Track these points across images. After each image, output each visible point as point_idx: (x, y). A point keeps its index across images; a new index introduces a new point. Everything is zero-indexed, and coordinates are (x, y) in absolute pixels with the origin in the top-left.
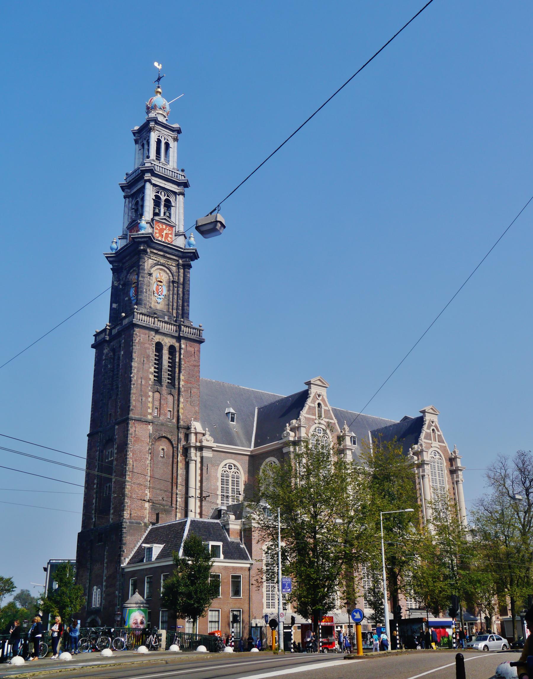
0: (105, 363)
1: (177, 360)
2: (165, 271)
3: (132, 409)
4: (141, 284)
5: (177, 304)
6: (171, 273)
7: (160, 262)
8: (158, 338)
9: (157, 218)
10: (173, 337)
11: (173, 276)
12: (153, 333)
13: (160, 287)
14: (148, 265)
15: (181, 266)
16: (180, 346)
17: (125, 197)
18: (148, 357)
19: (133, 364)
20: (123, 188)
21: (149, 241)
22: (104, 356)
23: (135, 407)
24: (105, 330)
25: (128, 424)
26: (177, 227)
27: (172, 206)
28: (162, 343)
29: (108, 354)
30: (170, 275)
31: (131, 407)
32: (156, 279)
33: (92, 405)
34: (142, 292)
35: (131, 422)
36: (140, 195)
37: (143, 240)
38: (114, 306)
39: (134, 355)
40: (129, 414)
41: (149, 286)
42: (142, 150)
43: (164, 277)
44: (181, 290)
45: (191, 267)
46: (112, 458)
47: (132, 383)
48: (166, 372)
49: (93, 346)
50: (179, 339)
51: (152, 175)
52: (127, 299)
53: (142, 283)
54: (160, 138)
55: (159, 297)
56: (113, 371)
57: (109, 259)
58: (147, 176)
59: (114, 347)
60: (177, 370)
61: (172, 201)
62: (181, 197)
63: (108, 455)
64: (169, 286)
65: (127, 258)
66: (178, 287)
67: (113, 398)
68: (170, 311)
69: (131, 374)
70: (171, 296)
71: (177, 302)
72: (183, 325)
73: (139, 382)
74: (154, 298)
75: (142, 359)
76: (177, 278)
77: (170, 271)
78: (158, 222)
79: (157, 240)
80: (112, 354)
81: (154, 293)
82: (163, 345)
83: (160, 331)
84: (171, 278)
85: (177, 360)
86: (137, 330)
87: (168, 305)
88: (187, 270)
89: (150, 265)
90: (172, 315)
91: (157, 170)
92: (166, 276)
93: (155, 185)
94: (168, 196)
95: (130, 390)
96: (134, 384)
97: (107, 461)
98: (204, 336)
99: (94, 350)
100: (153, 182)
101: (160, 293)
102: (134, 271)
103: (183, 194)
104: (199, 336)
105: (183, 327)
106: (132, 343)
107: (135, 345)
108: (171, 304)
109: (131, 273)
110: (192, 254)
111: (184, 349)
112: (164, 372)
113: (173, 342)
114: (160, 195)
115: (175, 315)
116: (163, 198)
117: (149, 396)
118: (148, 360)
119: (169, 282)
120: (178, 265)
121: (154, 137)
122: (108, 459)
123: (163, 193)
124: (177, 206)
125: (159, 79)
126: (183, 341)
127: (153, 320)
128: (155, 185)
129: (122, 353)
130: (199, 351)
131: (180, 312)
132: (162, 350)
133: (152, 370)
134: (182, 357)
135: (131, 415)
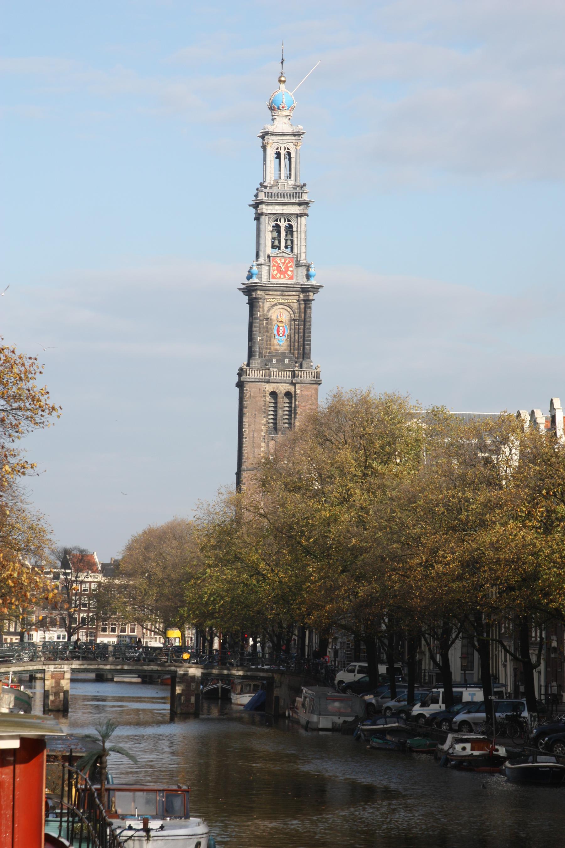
16: (295, 391)
19: (244, 420)
28: (277, 391)
30: (291, 312)
31: (244, 460)
41: (267, 332)
47: (245, 437)
54: (279, 150)
61: (294, 226)
64: (291, 325)
73: (251, 435)
84: (293, 315)
87: (290, 345)
89: (266, 309)
92: (288, 314)
96: (246, 438)
101: (281, 335)
107: (246, 401)
114: (278, 223)
116: (283, 224)
117: (262, 447)
123: (283, 220)
124: (299, 230)
131: (301, 351)
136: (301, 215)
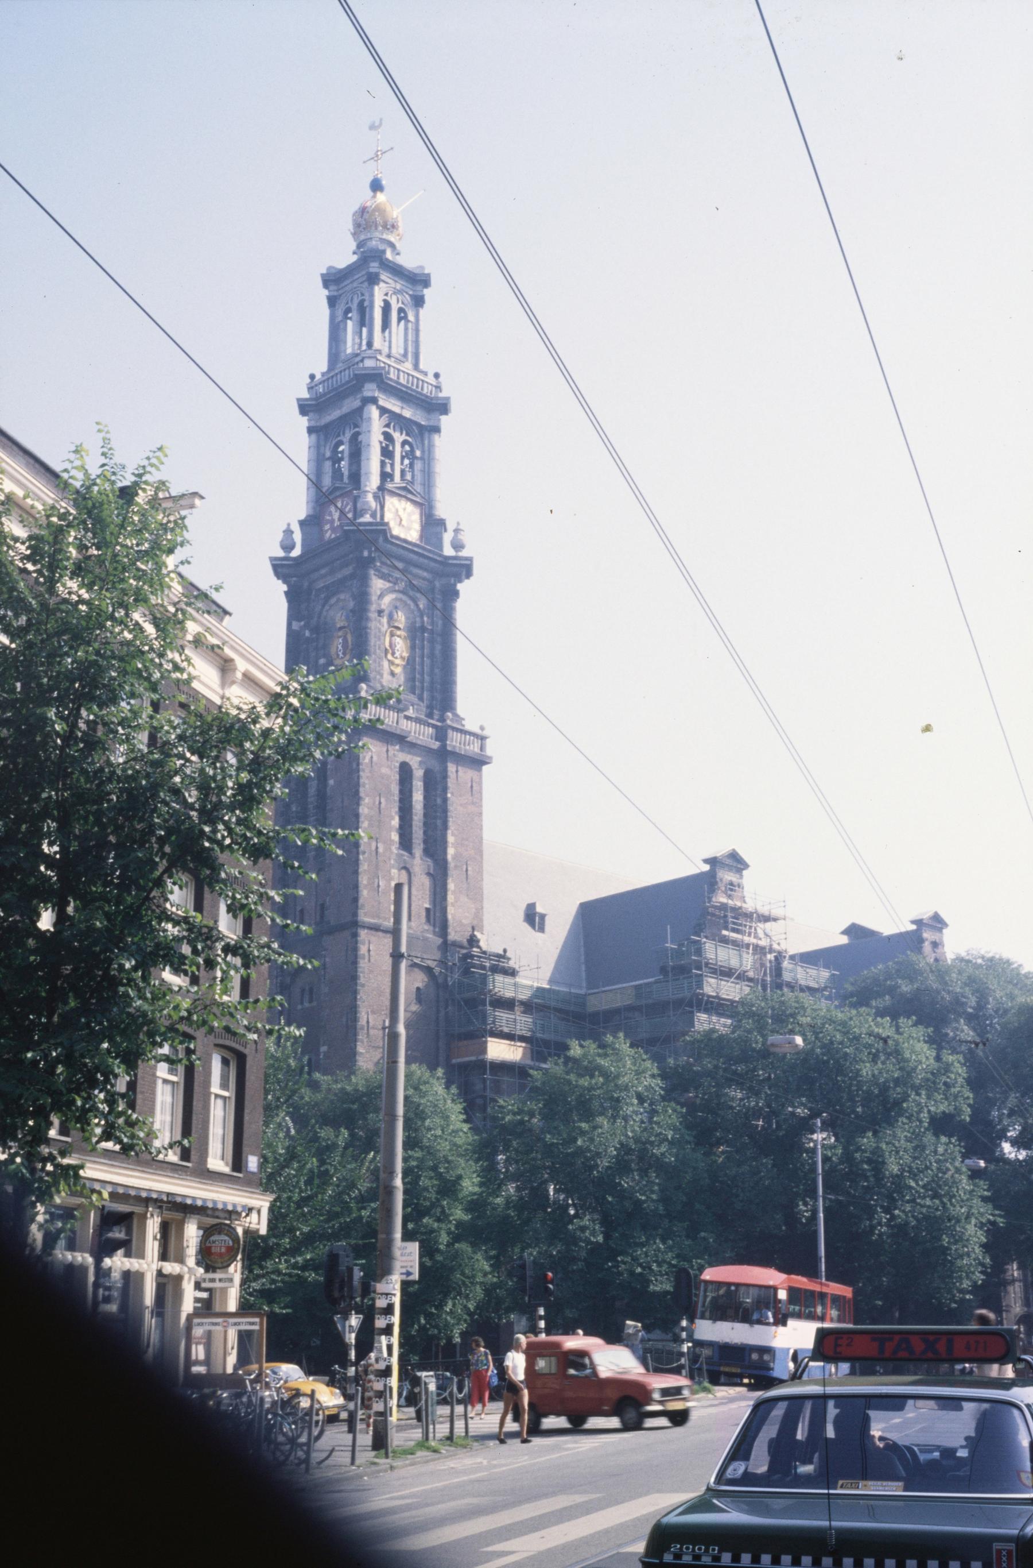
11: (422, 617)
17: (310, 430)
19: (361, 811)
20: (304, 408)
25: (355, 935)
35: (363, 934)
36: (347, 431)
47: (362, 848)
54: (388, 298)
73: (373, 848)
78: (393, 493)
83: (408, 739)
87: (413, 679)
93: (383, 411)
96: (364, 853)
97: (299, 1007)
100: (381, 403)
114: (391, 431)
116: (399, 437)
128: (383, 411)
133: (396, 822)
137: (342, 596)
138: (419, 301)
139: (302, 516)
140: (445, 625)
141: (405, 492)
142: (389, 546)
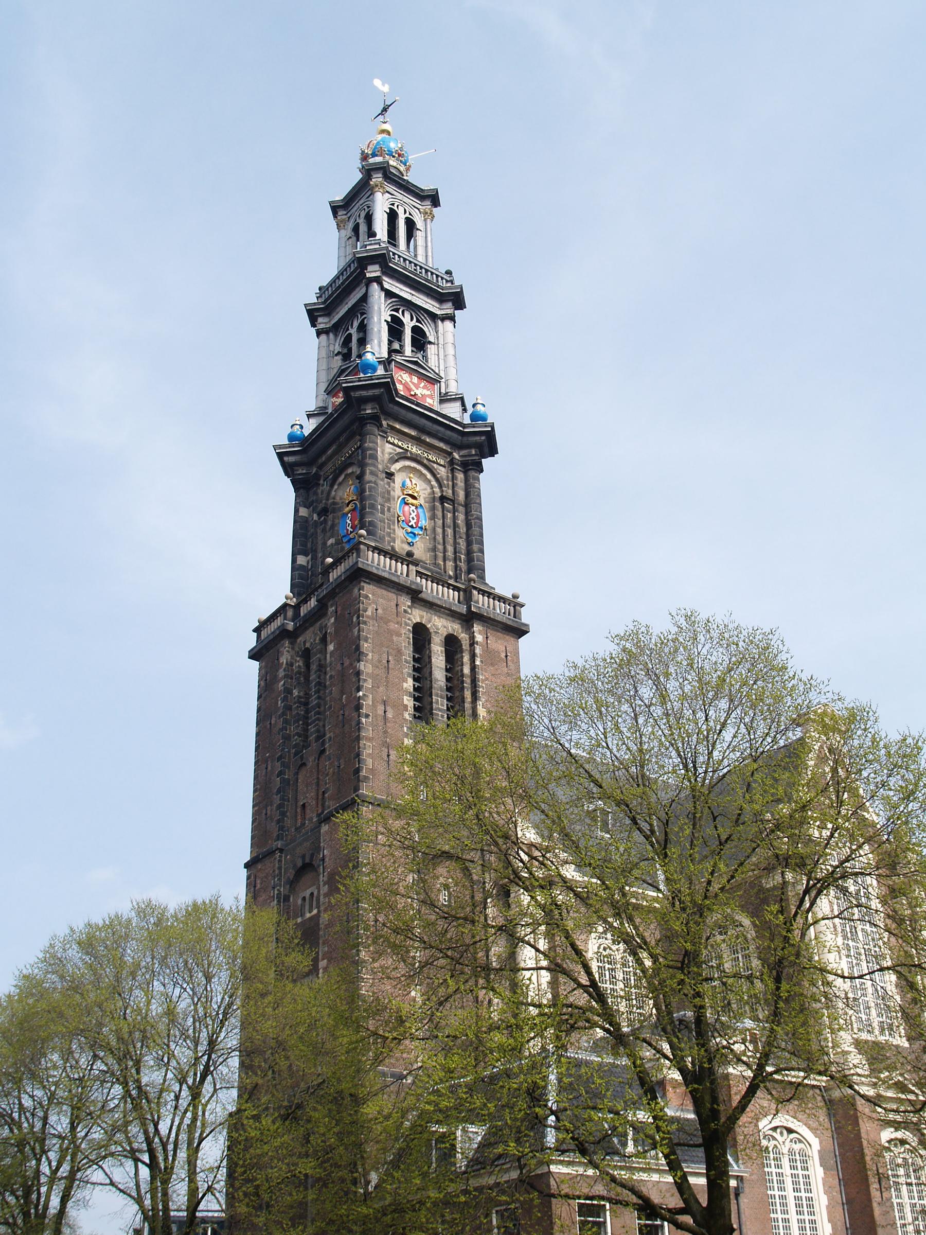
0: (284, 684)
1: (467, 670)
2: (421, 475)
3: (366, 778)
4: (370, 489)
5: (455, 549)
6: (437, 480)
7: (411, 453)
8: (418, 615)
9: (398, 358)
10: (452, 614)
12: (405, 601)
13: (413, 508)
14: (383, 453)
15: (457, 465)
16: (472, 638)
17: (319, 334)
18: (399, 652)
21: (386, 397)
22: (281, 670)
23: (372, 770)
24: (284, 608)
26: (443, 385)
27: (430, 343)
28: (429, 626)
29: (292, 665)
30: (434, 483)
31: (363, 773)
32: (403, 490)
33: (255, 791)
34: (373, 506)
37: (370, 393)
38: (302, 560)
39: (365, 646)
40: (357, 789)
41: (388, 500)
42: (354, 239)
43: (421, 488)
44: (461, 517)
45: (492, 450)
46: (315, 911)
47: (364, 711)
48: (441, 697)
49: (254, 655)
50: (469, 618)
51: (384, 273)
52: (331, 541)
53: (374, 488)
54: (395, 208)
55: (410, 530)
56: (306, 704)
57: (286, 459)
58: (373, 271)
59: (308, 645)
60: (468, 694)
62: (448, 324)
63: (303, 906)
64: (433, 509)
65: (330, 452)
66: (454, 511)
67: (310, 764)
68: (439, 564)
69: (358, 690)
70: (439, 530)
71: (455, 543)
72: (475, 588)
73: (380, 711)
74: (400, 533)
75: (385, 656)
76: (450, 491)
77: (434, 475)
79: (403, 397)
80: (301, 664)
81: (398, 521)
82: (431, 631)
83: (422, 595)
84: (437, 490)
85: (467, 670)
86: (369, 590)
87: (434, 549)
88: (472, 474)
89: (387, 456)
90: (445, 572)
91: (396, 264)
92: (424, 485)
93: (389, 294)
94: (418, 321)
95: (359, 730)
96: (367, 716)
98: (526, 616)
99: (256, 664)
102: (347, 476)
103: (452, 318)
104: (515, 617)
105: (475, 592)
106: (358, 617)
107: (365, 623)
108: (440, 547)
109: (340, 484)
110: (483, 438)
111: (481, 645)
112: (437, 695)
113: (454, 627)
114: (400, 315)
115: (451, 573)
116: (409, 323)
118: (398, 661)
119: (434, 499)
120: (452, 462)
121: (381, 203)
122: (302, 915)
123: (407, 315)
124: (441, 341)
125: (385, 110)
126: (477, 628)
127: (405, 567)
128: (389, 294)
129: (331, 647)
130: (517, 653)
132: (430, 643)
133: (409, 684)
134: (478, 663)
135: (364, 791)
136: (444, 318)
137: (350, 471)
138: (430, 216)
139: (312, 407)
140: (467, 495)
141: (418, 369)
142: (396, 408)
